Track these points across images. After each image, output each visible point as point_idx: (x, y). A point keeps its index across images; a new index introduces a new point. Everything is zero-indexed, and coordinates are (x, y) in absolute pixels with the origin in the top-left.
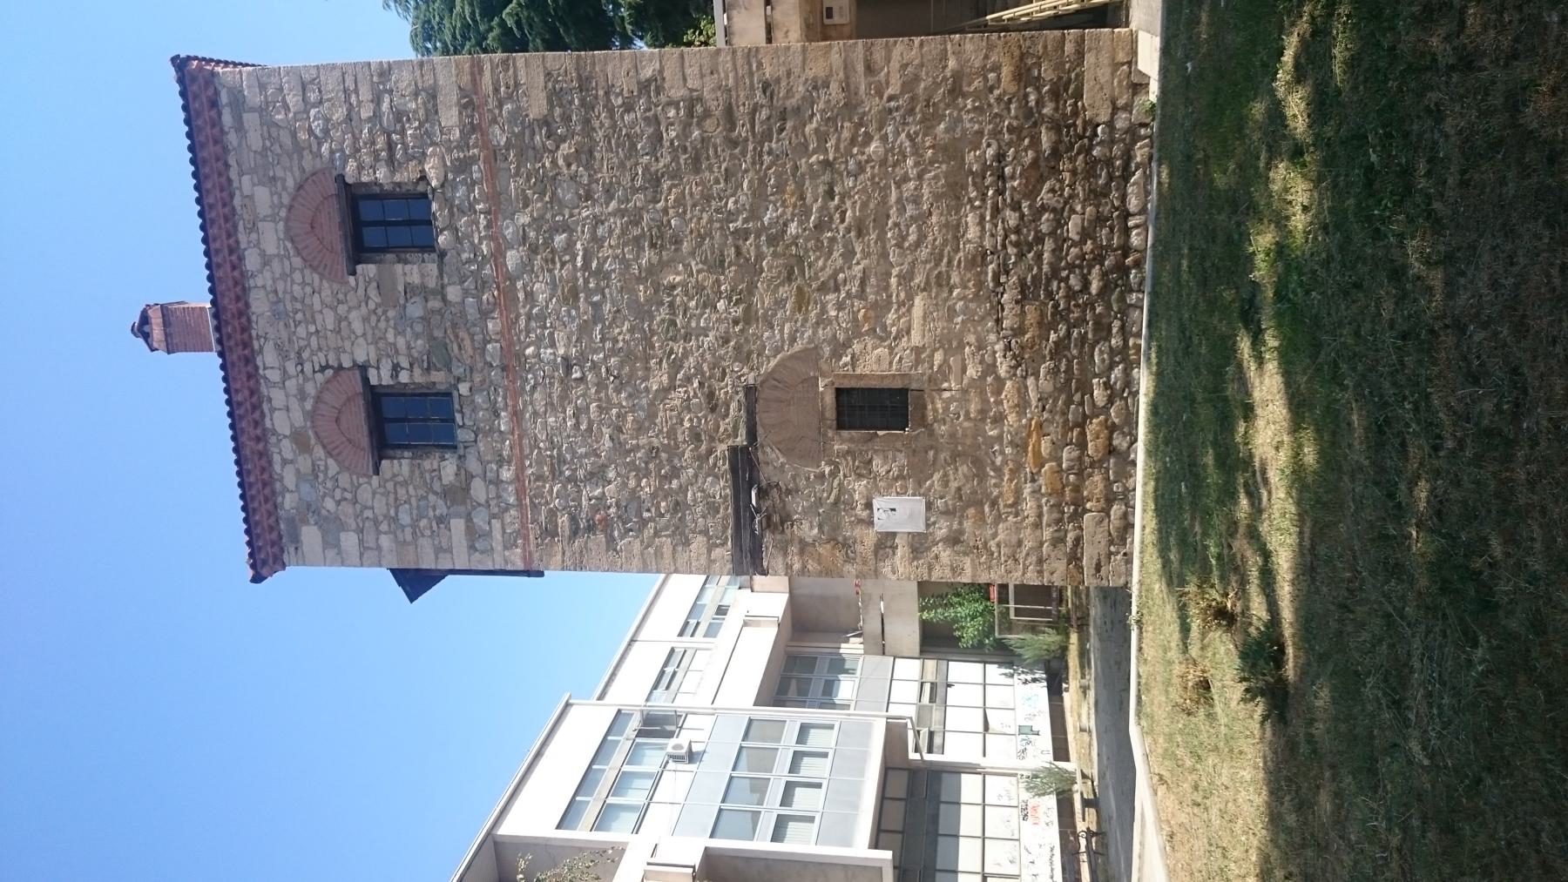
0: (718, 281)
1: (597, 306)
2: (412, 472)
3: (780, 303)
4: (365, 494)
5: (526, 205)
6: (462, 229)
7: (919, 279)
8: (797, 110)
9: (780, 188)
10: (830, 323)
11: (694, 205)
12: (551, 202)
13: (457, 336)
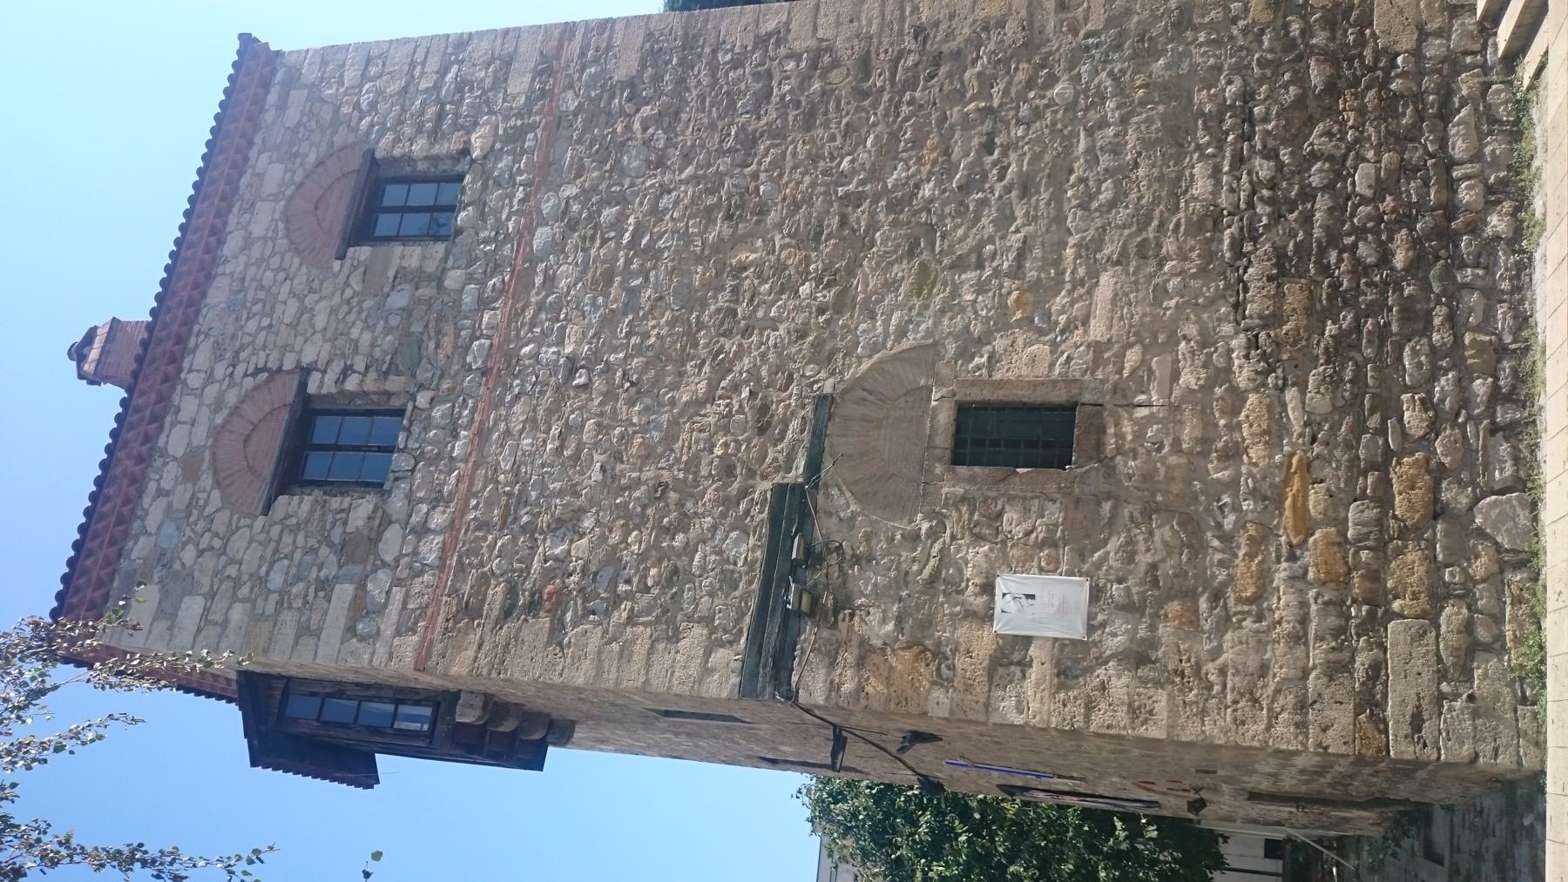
0: (807, 258)
1: (633, 293)
2: (312, 512)
3: (891, 286)
4: (238, 544)
5: (579, 176)
6: (491, 212)
7: (1110, 249)
8: (957, 55)
9: (917, 143)
10: (963, 310)
11: (795, 167)
12: (611, 171)
13: (439, 332)
